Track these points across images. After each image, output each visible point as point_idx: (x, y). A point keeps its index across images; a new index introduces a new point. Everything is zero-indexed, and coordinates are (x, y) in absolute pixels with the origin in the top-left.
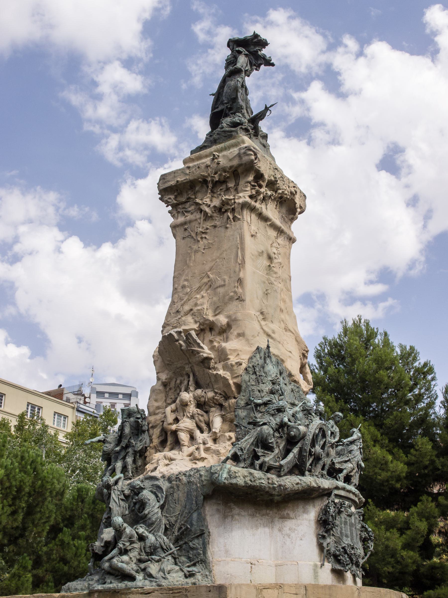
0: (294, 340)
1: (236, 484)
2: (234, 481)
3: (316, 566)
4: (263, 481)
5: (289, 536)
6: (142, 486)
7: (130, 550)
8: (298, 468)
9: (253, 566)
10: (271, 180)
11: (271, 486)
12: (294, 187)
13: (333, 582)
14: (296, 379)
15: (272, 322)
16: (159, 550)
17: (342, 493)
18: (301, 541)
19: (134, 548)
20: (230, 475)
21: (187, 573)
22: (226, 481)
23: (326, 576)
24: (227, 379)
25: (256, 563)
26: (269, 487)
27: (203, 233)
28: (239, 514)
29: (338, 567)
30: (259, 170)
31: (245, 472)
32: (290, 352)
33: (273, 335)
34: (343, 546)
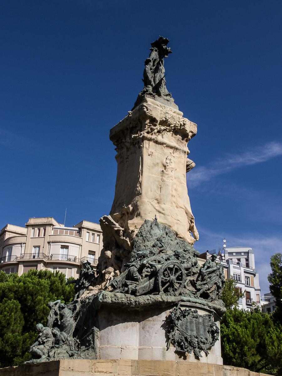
0: (185, 213)
1: (106, 302)
2: (105, 300)
3: (164, 349)
4: (123, 299)
5: (148, 331)
6: (64, 306)
7: (46, 342)
8: (155, 290)
9: (122, 350)
10: (163, 120)
11: (129, 302)
12: (183, 121)
13: (176, 359)
14: (180, 236)
15: (164, 204)
16: (61, 341)
17: (188, 304)
18: (156, 335)
19: (48, 341)
20: (103, 297)
21: (71, 354)
22: (101, 301)
23: (171, 355)
24: (127, 241)
25: (125, 348)
26: (128, 303)
27: (127, 158)
28: (116, 320)
29: (179, 349)
30: (152, 116)
31: (111, 294)
32: (178, 220)
33: (163, 212)
34: (185, 336)
